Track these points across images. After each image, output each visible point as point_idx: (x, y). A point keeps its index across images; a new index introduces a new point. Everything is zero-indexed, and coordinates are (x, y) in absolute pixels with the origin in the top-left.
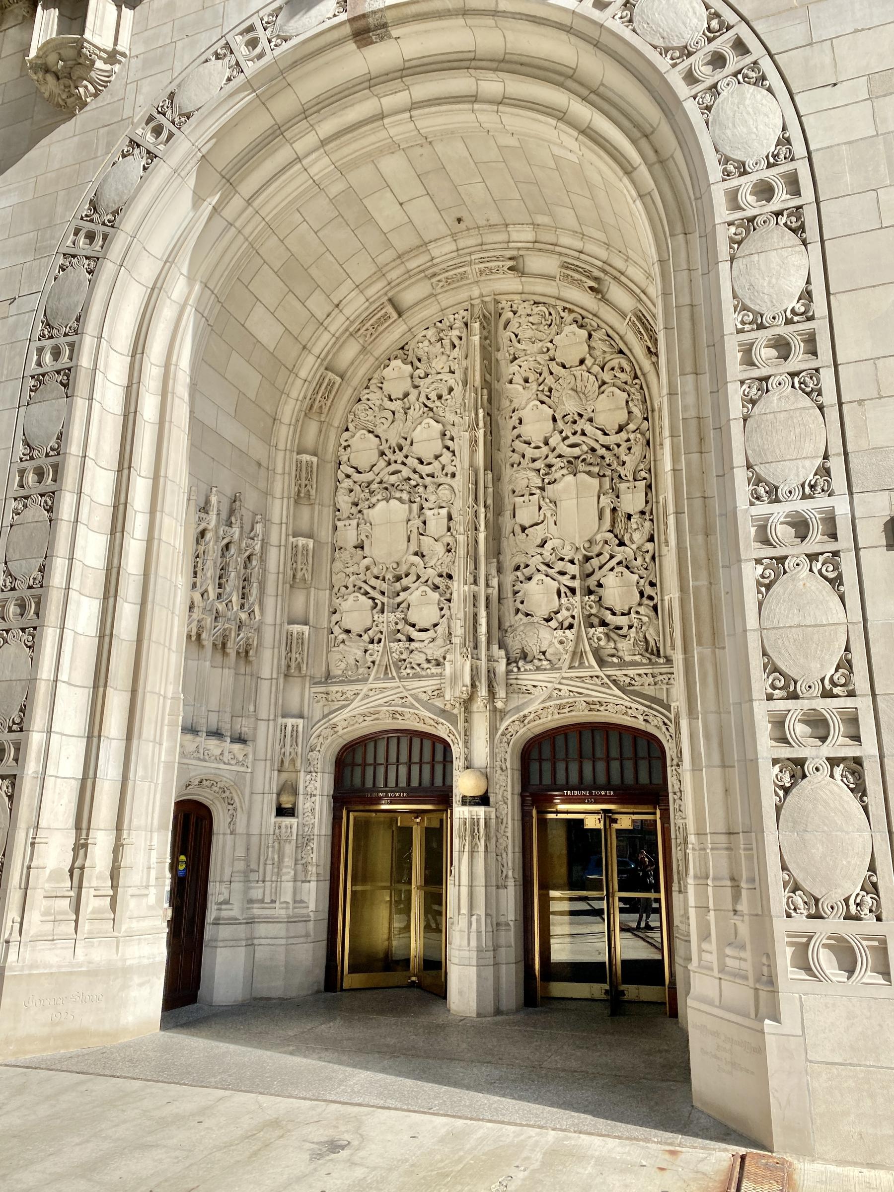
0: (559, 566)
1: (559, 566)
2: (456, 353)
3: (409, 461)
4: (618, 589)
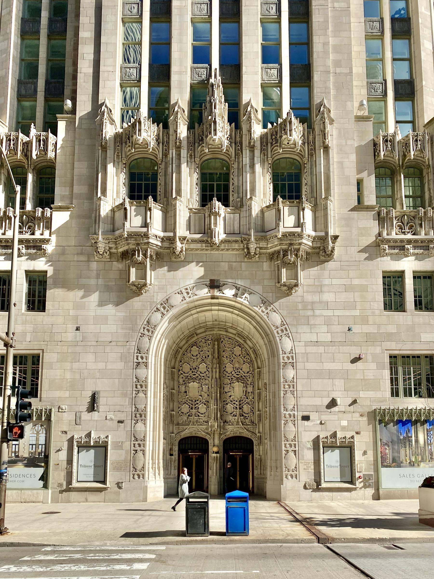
0: (234, 402)
1: (234, 402)
2: (210, 347)
3: (198, 372)
4: (246, 408)
